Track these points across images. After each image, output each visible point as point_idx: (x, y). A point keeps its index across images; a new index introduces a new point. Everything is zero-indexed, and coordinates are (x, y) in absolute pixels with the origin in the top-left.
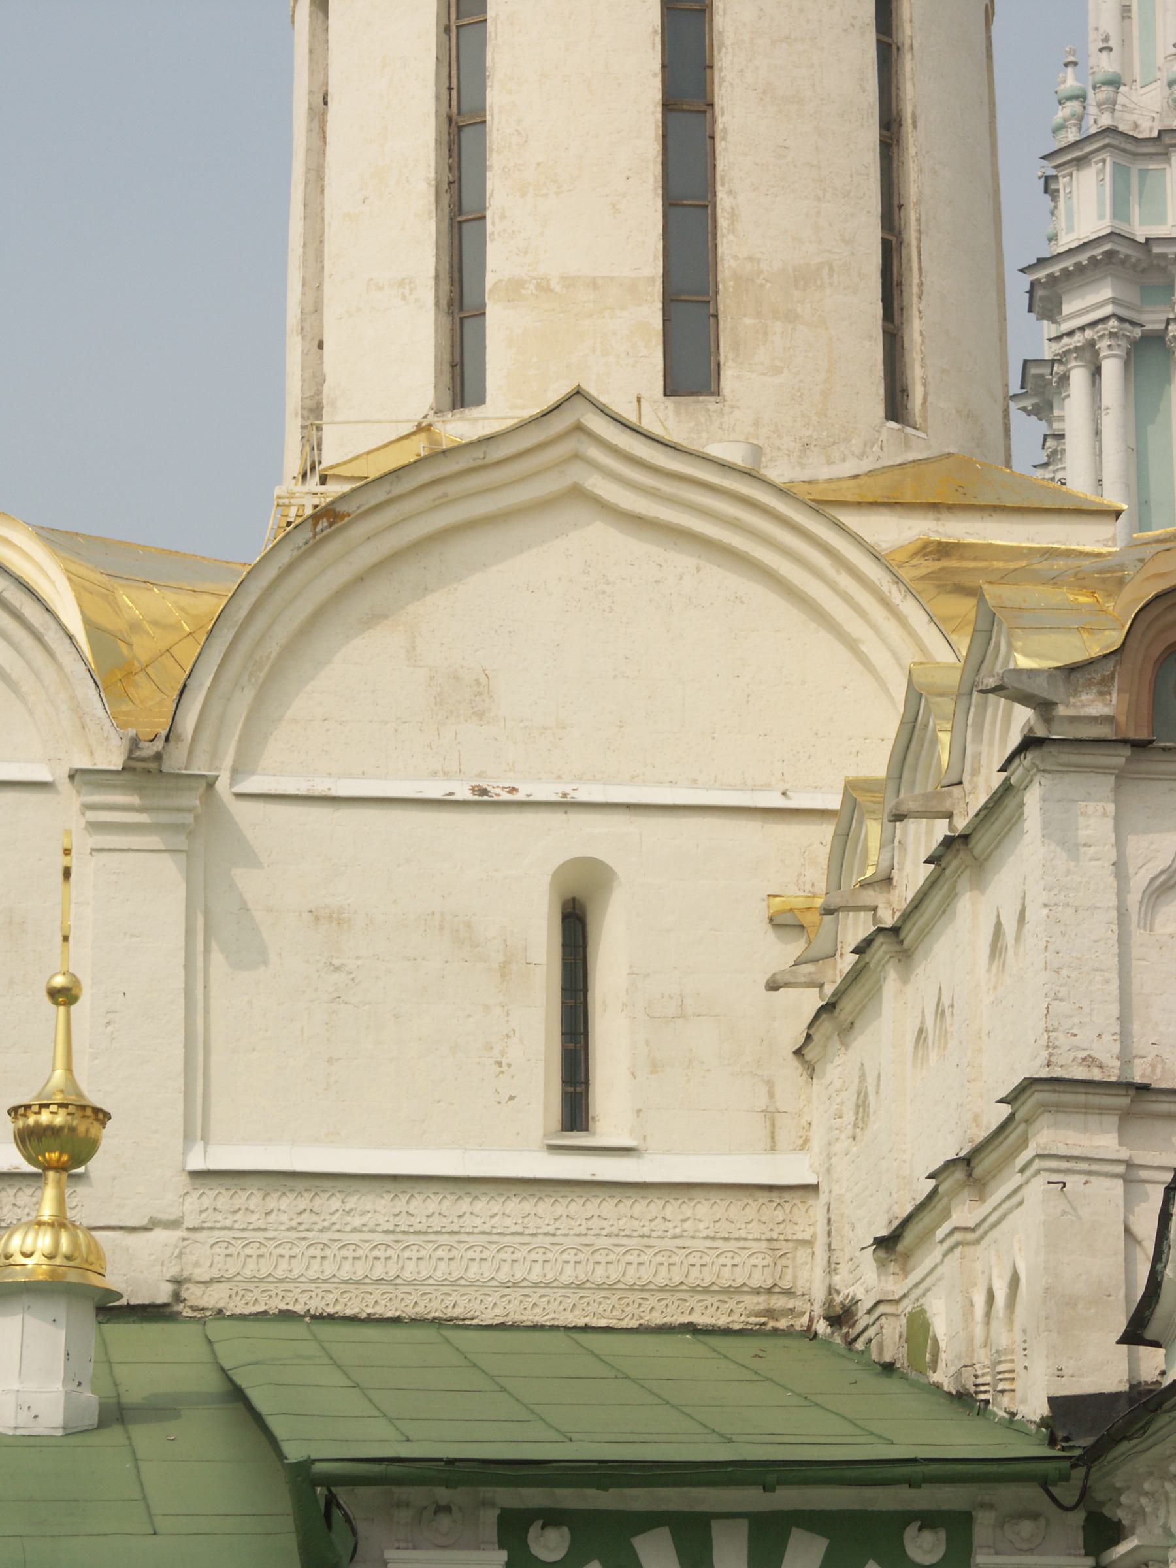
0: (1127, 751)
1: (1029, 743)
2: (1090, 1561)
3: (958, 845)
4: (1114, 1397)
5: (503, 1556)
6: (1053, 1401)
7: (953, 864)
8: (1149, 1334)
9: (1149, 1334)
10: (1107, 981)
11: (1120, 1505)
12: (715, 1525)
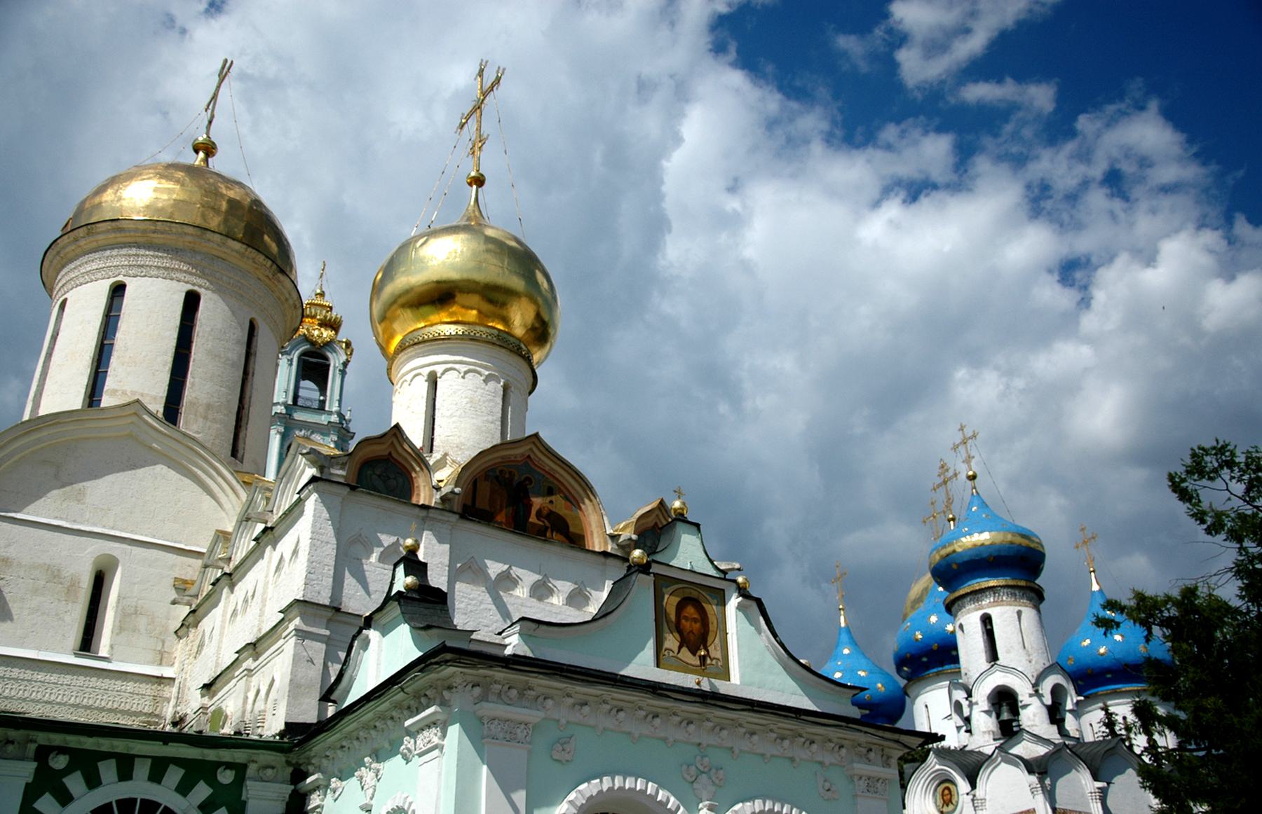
0: (348, 489)
1: (313, 480)
2: (292, 787)
3: (269, 531)
4: (311, 725)
5: (35, 765)
6: (286, 724)
7: (265, 539)
8: (332, 698)
9: (332, 698)
10: (329, 570)
11: (310, 764)
12: (136, 759)
